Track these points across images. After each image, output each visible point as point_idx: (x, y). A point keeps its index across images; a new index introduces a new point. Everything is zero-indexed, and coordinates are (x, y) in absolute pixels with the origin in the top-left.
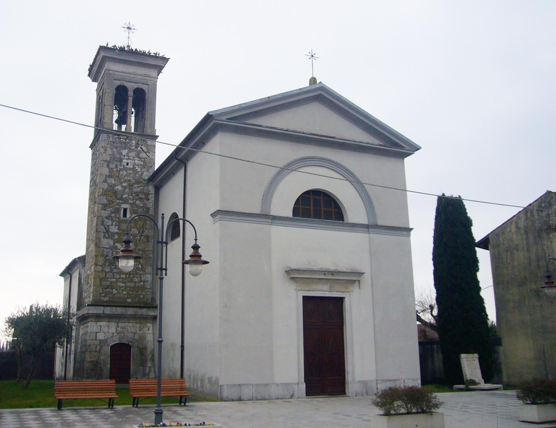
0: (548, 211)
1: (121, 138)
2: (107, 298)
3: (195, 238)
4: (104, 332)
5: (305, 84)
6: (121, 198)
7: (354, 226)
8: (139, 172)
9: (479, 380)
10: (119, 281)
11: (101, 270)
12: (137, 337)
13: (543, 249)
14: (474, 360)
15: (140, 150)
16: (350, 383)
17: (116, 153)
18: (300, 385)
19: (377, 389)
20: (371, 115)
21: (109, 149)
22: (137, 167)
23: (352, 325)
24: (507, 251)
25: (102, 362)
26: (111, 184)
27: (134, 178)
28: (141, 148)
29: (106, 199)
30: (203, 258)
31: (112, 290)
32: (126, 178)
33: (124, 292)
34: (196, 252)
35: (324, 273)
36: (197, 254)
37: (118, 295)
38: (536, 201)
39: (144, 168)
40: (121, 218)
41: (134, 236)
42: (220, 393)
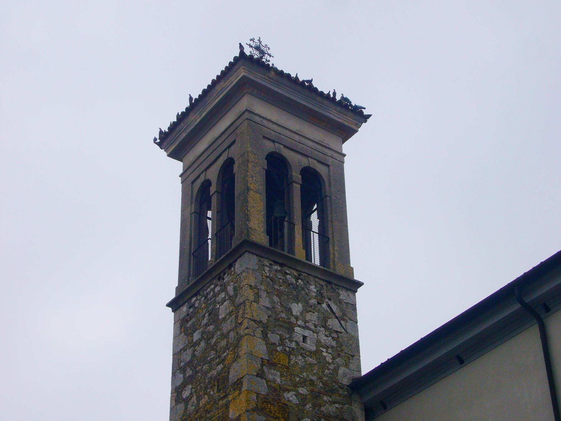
1: (287, 274)
8: (329, 364)
22: (324, 350)
26: (274, 385)
28: (329, 306)
39: (339, 355)
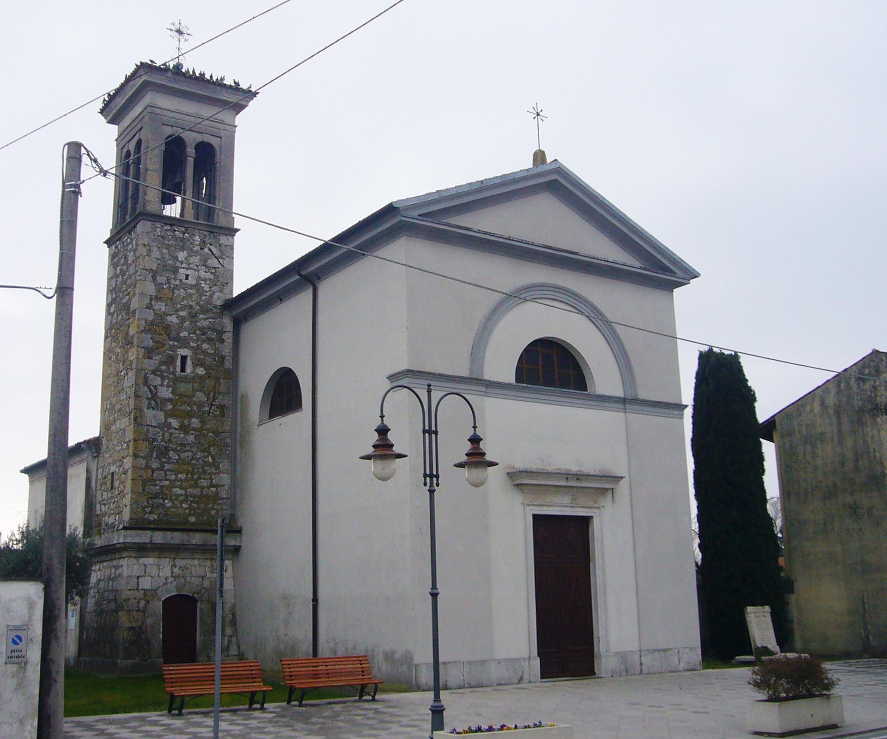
0: (875, 382)
1: (175, 231)
2: (154, 516)
3: (473, 425)
4: (151, 576)
5: (528, 164)
6: (177, 338)
7: (604, 400)
8: (207, 292)
9: (774, 647)
10: (175, 485)
11: (144, 466)
12: (206, 583)
13: (865, 441)
14: (765, 616)
15: (208, 254)
16: (602, 656)
17: (167, 257)
18: (531, 661)
19: (641, 664)
20: (630, 219)
21: (155, 249)
22: (203, 282)
23: (603, 562)
24: (806, 442)
25: (149, 630)
26: (159, 312)
27: (198, 303)
28: (210, 250)
29: (151, 338)
30: (488, 458)
31: (164, 501)
32: (185, 302)
33: (185, 506)
34: (475, 448)
35: (566, 476)
36: (478, 452)
37: (173, 510)
38: (855, 364)
39: (215, 285)
40: (177, 374)
41: (200, 405)
42: (416, 677)
